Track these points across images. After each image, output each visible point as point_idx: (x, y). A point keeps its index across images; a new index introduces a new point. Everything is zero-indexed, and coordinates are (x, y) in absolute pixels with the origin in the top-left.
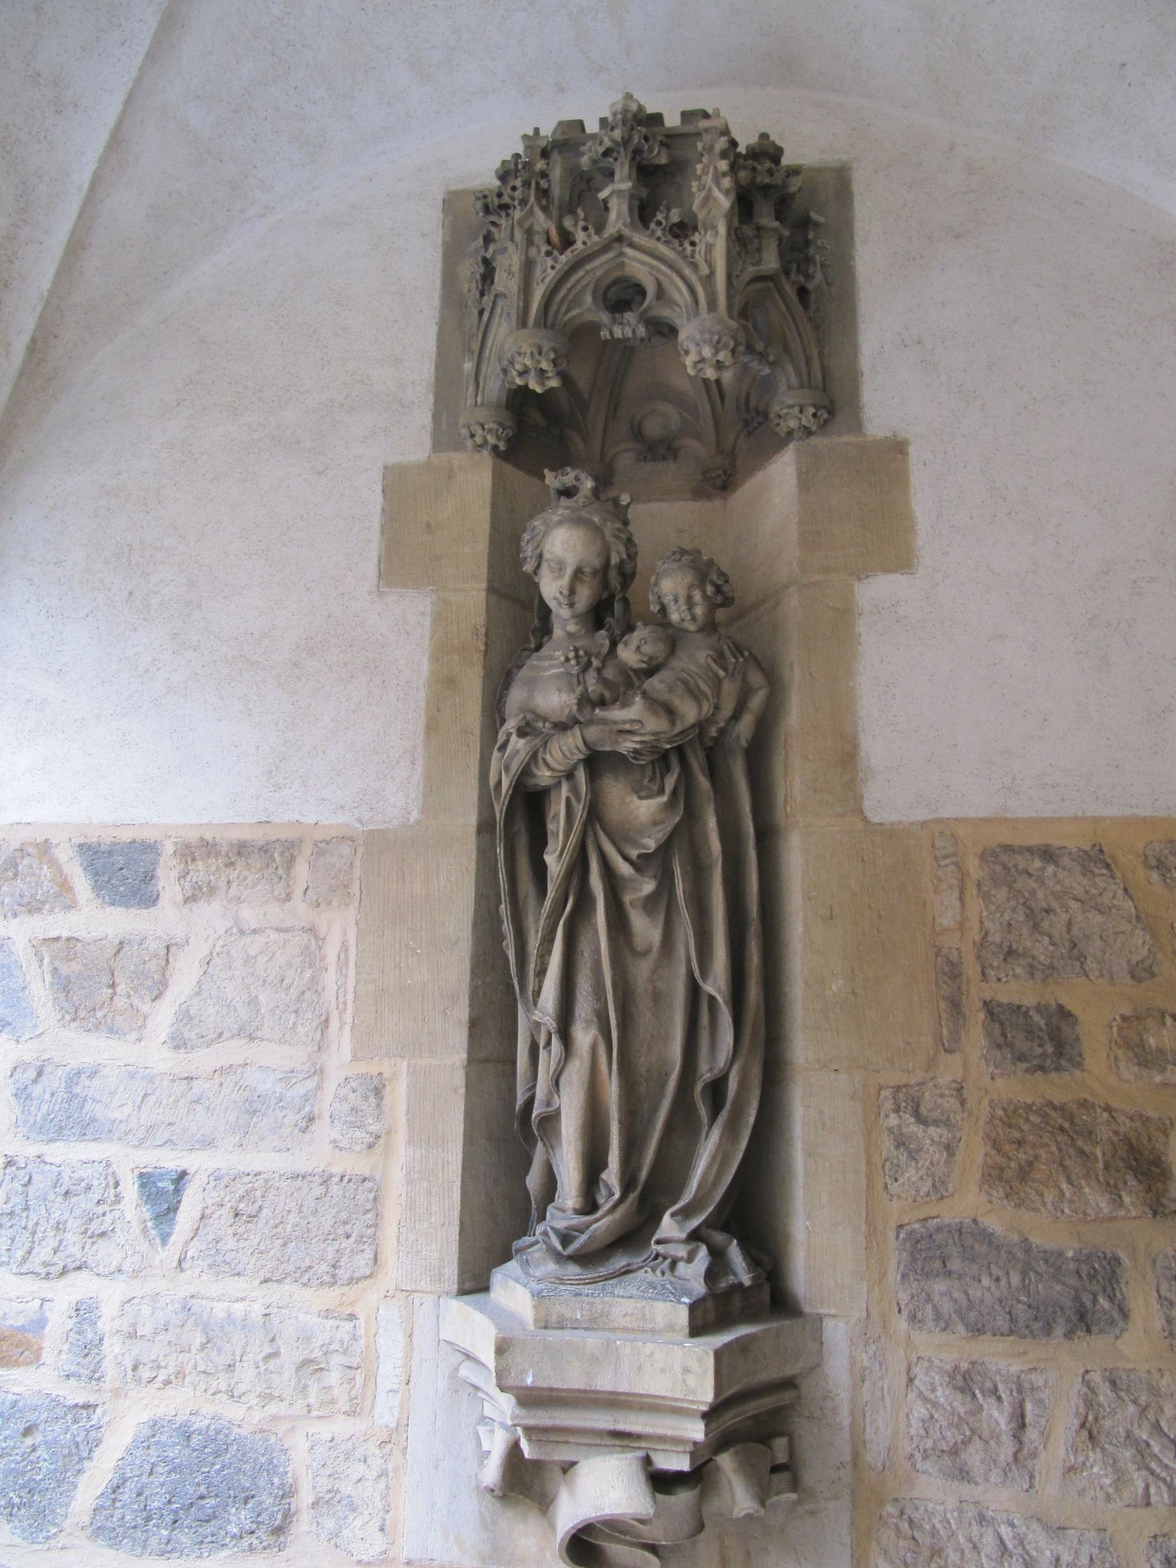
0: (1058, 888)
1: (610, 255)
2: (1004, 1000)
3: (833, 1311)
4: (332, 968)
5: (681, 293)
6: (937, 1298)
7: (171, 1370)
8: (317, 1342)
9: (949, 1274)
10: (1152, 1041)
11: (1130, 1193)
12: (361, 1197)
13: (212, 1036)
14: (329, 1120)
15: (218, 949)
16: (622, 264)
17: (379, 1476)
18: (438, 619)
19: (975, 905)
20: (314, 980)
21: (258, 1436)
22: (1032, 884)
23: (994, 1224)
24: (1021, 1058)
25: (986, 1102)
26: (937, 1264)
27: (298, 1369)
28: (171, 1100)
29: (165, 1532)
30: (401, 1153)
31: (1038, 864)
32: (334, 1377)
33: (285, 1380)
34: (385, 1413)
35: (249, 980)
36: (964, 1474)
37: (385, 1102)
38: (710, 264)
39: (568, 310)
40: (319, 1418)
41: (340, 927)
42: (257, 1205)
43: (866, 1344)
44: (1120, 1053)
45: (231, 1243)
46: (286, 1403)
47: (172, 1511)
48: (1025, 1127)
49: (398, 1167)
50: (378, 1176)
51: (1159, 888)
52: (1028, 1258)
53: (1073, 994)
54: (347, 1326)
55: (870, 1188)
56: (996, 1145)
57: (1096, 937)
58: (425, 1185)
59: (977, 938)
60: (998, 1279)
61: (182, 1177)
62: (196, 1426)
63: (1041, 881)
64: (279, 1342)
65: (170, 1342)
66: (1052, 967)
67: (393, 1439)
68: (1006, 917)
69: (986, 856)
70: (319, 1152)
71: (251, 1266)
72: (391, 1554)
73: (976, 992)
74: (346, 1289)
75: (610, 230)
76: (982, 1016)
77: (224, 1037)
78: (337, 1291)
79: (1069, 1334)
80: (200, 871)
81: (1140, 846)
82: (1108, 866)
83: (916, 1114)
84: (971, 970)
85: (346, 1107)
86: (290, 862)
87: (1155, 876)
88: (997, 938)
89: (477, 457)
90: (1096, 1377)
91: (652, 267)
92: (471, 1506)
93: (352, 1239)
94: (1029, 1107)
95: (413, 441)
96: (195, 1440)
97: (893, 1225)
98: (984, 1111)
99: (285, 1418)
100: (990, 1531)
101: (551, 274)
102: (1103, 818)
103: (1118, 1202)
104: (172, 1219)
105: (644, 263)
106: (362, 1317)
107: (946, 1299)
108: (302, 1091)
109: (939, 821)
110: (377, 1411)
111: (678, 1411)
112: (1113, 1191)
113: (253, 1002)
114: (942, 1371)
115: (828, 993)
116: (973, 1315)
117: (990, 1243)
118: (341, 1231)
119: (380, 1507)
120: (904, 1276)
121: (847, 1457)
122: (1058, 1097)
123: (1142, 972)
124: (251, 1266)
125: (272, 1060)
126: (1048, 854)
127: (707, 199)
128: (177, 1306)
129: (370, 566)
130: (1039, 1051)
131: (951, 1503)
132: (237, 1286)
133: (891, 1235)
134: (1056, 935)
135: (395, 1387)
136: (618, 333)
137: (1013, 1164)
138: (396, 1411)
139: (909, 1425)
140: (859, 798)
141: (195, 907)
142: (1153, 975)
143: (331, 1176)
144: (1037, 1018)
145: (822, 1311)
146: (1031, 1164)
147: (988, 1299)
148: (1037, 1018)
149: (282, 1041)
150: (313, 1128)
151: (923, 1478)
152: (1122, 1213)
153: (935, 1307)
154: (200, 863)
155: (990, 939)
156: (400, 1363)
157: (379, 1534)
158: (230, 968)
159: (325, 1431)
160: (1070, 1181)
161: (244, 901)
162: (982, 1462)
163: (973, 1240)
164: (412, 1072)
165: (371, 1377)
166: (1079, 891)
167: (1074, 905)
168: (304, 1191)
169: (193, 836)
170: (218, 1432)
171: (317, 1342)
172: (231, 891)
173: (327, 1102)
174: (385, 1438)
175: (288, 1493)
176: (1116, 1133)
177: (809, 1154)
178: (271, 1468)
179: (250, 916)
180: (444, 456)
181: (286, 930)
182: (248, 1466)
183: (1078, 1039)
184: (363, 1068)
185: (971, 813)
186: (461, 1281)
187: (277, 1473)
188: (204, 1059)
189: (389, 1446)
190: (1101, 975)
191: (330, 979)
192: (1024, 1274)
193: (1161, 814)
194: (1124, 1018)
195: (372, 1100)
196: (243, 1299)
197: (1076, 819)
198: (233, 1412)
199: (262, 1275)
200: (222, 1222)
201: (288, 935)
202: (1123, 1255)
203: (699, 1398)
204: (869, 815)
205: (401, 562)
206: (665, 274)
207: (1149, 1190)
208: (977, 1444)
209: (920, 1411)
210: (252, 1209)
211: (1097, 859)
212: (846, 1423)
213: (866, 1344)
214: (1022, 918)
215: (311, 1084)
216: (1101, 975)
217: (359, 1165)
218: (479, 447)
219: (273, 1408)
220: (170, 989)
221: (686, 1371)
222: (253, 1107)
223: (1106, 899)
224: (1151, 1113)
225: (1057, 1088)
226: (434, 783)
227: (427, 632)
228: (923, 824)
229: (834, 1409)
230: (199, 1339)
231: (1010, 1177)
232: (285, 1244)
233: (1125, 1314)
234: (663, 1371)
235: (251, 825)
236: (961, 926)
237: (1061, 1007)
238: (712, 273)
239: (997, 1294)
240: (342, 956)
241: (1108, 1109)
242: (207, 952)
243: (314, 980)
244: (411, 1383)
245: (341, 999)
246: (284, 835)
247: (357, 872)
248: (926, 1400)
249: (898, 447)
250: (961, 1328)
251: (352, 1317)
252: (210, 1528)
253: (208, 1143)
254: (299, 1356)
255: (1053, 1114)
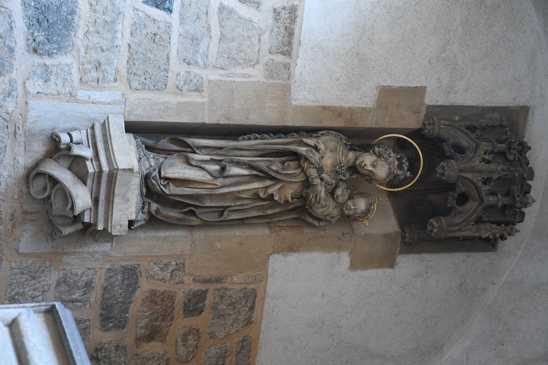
0: (241, 311)
1: (477, 197)
2: (208, 295)
3: (113, 246)
4: (242, 71)
5: (458, 220)
6: (116, 277)
7: (97, 7)
8: (107, 68)
9: (124, 280)
10: (190, 337)
11: (144, 332)
12: (159, 84)
13: (222, 24)
14: (188, 70)
15: (255, 25)
16: (473, 200)
17: (58, 92)
18: (364, 110)
19: (239, 287)
20: (239, 64)
21: (71, 43)
22: (243, 304)
23: (138, 293)
24: (189, 300)
25: (176, 290)
26: (126, 276)
27: (97, 60)
28: (200, 6)
29: (33, 4)
30: (174, 100)
31: (249, 305)
32: (94, 74)
33: (94, 56)
34: (82, 94)
35: (242, 38)
36: (58, 284)
37: (193, 93)
38: (465, 230)
39: (462, 183)
40: (79, 68)
41: (257, 74)
42: (158, 42)
43: (102, 256)
44: (188, 329)
45: (144, 32)
46: (84, 55)
47: (42, 7)
48: (167, 302)
49: (168, 98)
50: (166, 90)
51: (237, 340)
52: (127, 303)
53: (207, 314)
54: (112, 79)
55: (152, 256)
56: (163, 293)
57: (224, 322)
58: (163, 109)
59: (228, 288)
60: (121, 295)
61: (170, 11)
62: (75, 17)
63: (244, 306)
64: (108, 51)
65: (107, 7)
66: (217, 309)
67: (72, 96)
68: (234, 296)
69: (254, 291)
70: (176, 67)
71: (135, 40)
72: (29, 96)
73: (211, 287)
74: (126, 78)
75: (485, 198)
76: (204, 289)
77: (222, 28)
78: (125, 74)
79: (101, 315)
80: (284, 15)
81: (251, 335)
82: (246, 326)
83: (175, 270)
84: (219, 286)
85: (192, 78)
86: (283, 53)
87: (241, 339)
88: (228, 293)
89: (421, 122)
90: (88, 323)
91: (470, 210)
92: (47, 125)
93: (144, 81)
94: (173, 303)
95: (434, 98)
96: (69, 17)
97: (140, 263)
98: (172, 290)
99: (79, 55)
100: (40, 294)
101: (475, 180)
102: (261, 324)
103: (142, 328)
104: (153, 5)
105: (471, 208)
106: (116, 84)
107: (115, 279)
108: (199, 61)
109: (267, 277)
110: (82, 91)
111: (106, 221)
112: (146, 327)
113: (233, 40)
114: (92, 278)
115: (216, 243)
116: (110, 288)
117: (132, 292)
118: (148, 77)
119: (47, 92)
120: (123, 266)
121: (66, 251)
122: (175, 311)
123: (212, 335)
124: (135, 40)
125: (212, 47)
126: (252, 308)
127: (487, 230)
128: (121, 10)
129: (389, 82)
130: (191, 305)
131: (50, 282)
132: (127, 34)
133: (136, 263)
134: (226, 311)
135: (91, 98)
136: (451, 198)
137: (156, 298)
138: (82, 98)
139: (75, 269)
140: (278, 253)
141: (272, 12)
142: (210, 338)
143: (167, 72)
144: (201, 305)
145: (114, 242)
146: (156, 303)
147: (114, 292)
148: (201, 305)
149: (218, 52)
150: (185, 64)
151: (57, 273)
152: (138, 329)
153: (113, 276)
154: (288, 16)
155: (228, 291)
156: (100, 100)
157: (36, 92)
158: (247, 30)
159: (74, 71)
160: (150, 315)
161: (271, 34)
162: (62, 290)
163: (134, 286)
164: (203, 104)
165: (95, 89)
166: (239, 317)
167: (235, 316)
168: (162, 61)
169: (299, 13)
170: (73, 27)
171: (107, 68)
172: (276, 28)
173: (194, 70)
174: (73, 94)
175: (50, 55)
176: (163, 328)
177: (165, 238)
178: (59, 49)
179: (266, 37)
180: (424, 110)
181: (258, 53)
182: (60, 39)
183: (193, 316)
184: (206, 84)
185: (268, 286)
186: (127, 122)
187: (58, 51)
188: (214, 21)
189: (69, 96)
190: (212, 323)
191: (239, 70)
192: (122, 302)
193: (260, 341)
194: (198, 330)
195: (194, 88)
196: (122, 36)
197: (262, 317)
198: (80, 34)
199: (132, 44)
200: (152, 29)
201: (257, 54)
202: (125, 330)
203: (113, 230)
204: (272, 256)
205: (387, 93)
206: (466, 215)
207: (144, 337)
208: (68, 289)
209: (80, 272)
210: (156, 41)
211: (249, 322)
212: (77, 250)
213: (102, 256)
214: (233, 301)
215: (201, 64)
216: (212, 323)
217: (171, 84)
218: (424, 125)
219: (83, 50)
220: (242, 5)
221: (121, 226)
222: (195, 40)
223: (236, 325)
224: (168, 337)
225: (178, 310)
226: (304, 110)
227: (360, 106)
228: (267, 272)
229: (81, 247)
230: (108, 19)
231: (153, 297)
232: (143, 54)
233: (107, 330)
234: (120, 218)
235: (300, 38)
236: (234, 283)
237: (203, 311)
238: (462, 231)
239: (116, 294)
240: (247, 76)
241: (171, 325)
242: (254, 20)
243: (239, 64)
244: (92, 104)
245: (231, 75)
246: (294, 51)
247: (276, 81)
248: (83, 274)
249: (392, 265)
250: (106, 284)
251: (116, 80)
252: (35, 22)
253: (182, 20)
254: (102, 60)
255: (170, 310)
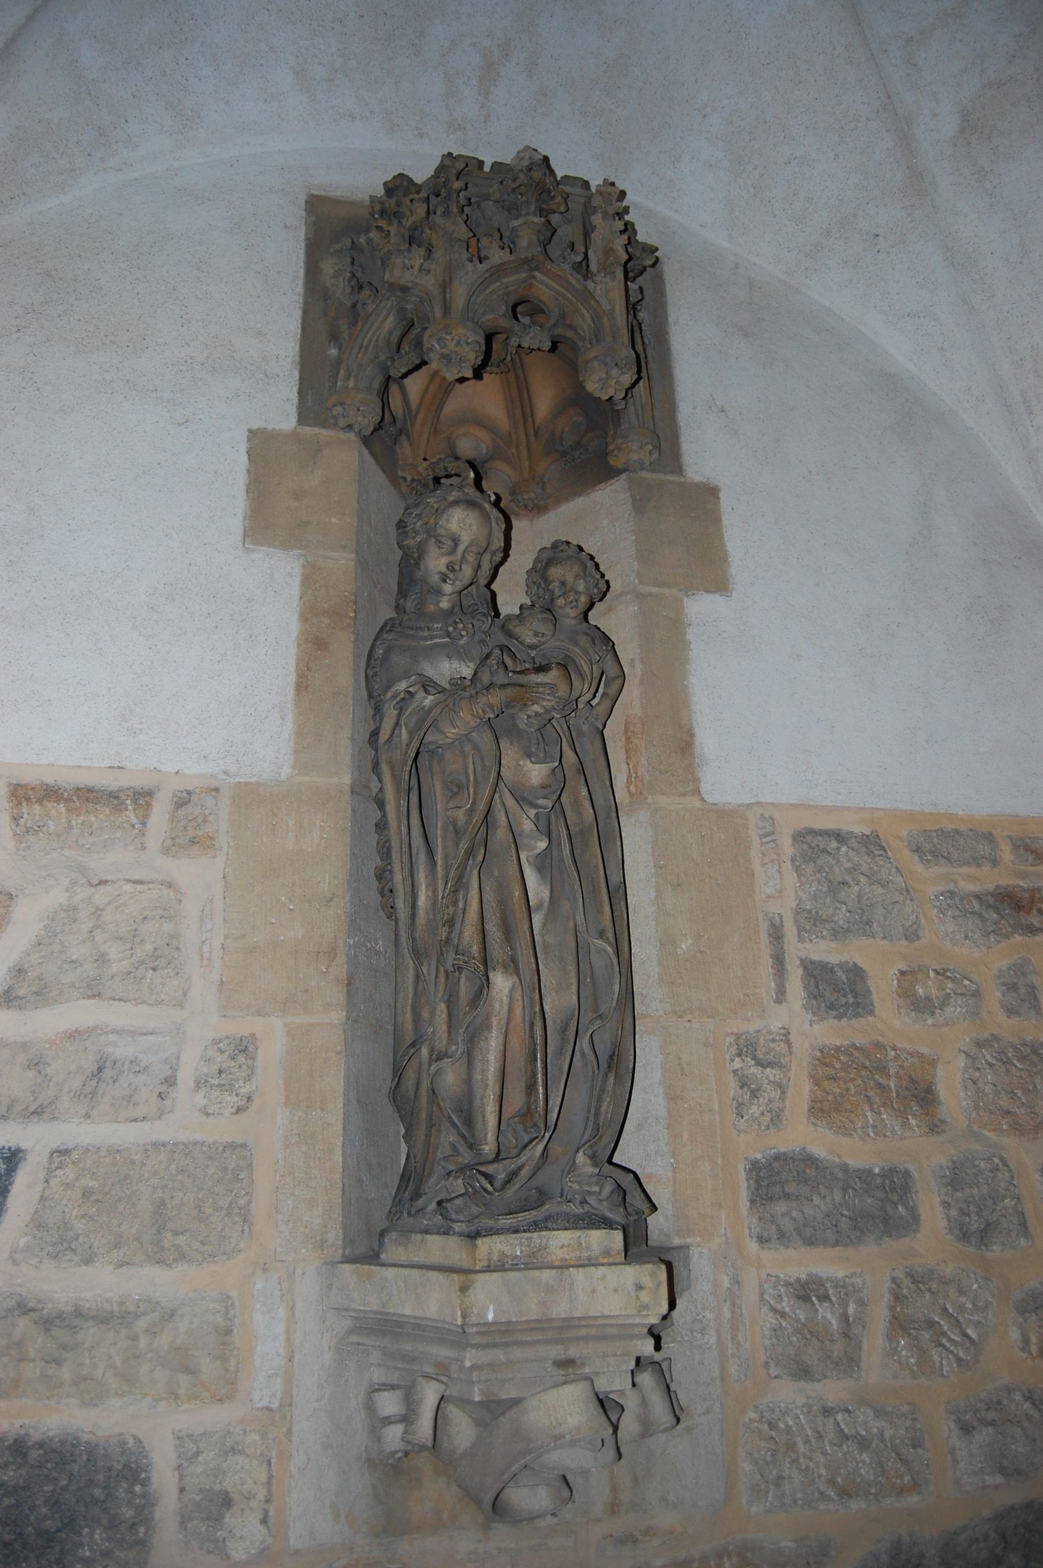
0: (849, 865)
10: (921, 991)
11: (914, 1116)
18: (307, 581)
19: (791, 878)
22: (832, 861)
24: (831, 1007)
48: (837, 1065)
56: (817, 1083)
59: (794, 905)
73: (795, 949)
76: (800, 971)
82: (883, 849)
83: (755, 1058)
84: (790, 931)
91: (557, 292)
94: (838, 1049)
95: (279, 408)
100: (831, 1420)
103: (905, 1124)
112: (902, 1114)
113: (102, 959)
117: (817, 1167)
121: (716, 1373)
126: (839, 837)
130: (843, 1001)
140: (697, 780)
157: (261, 1528)
160: (872, 1110)
166: (865, 868)
167: (863, 879)
169: (29, 778)
176: (902, 1067)
180: (308, 431)
192: (844, 1190)
193: (917, 808)
194: (902, 973)
202: (911, 1168)
204: (706, 797)
205: (264, 524)
211: (872, 843)
221: (639, 1287)
234: (616, 1291)
241: (894, 1048)
245: (206, 955)
248: (774, 1310)
249: (711, 492)
255: (855, 1053)
